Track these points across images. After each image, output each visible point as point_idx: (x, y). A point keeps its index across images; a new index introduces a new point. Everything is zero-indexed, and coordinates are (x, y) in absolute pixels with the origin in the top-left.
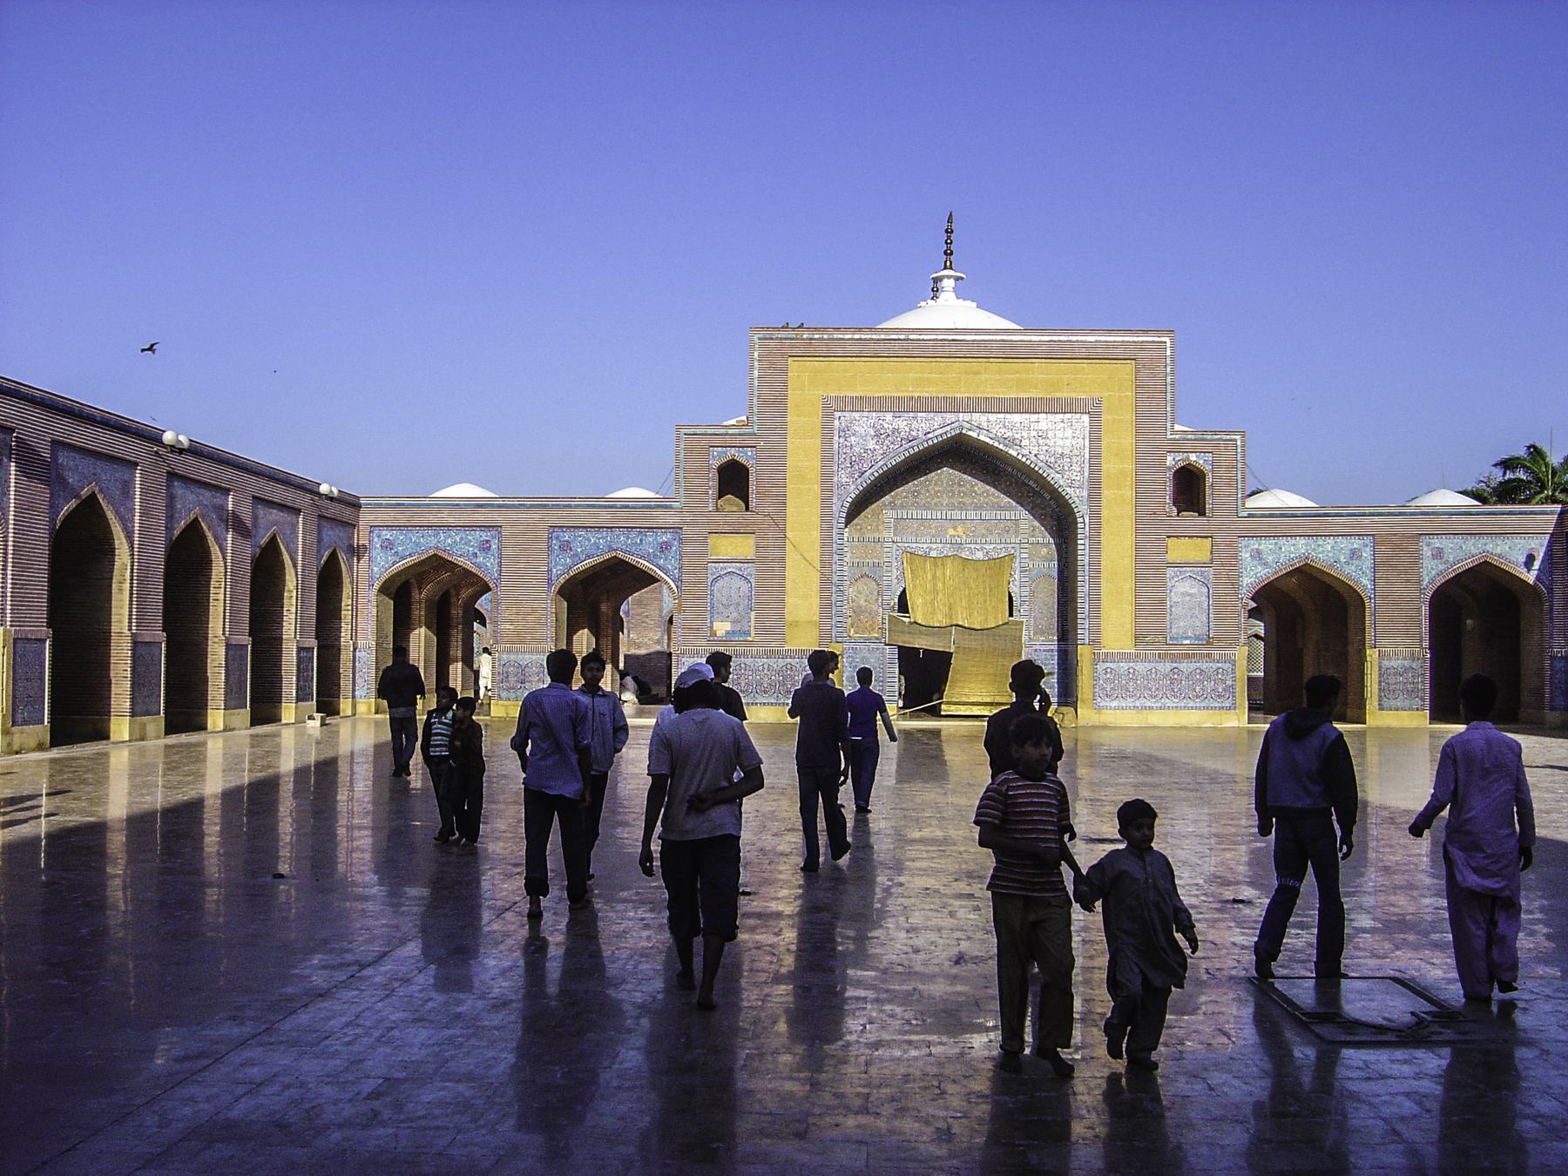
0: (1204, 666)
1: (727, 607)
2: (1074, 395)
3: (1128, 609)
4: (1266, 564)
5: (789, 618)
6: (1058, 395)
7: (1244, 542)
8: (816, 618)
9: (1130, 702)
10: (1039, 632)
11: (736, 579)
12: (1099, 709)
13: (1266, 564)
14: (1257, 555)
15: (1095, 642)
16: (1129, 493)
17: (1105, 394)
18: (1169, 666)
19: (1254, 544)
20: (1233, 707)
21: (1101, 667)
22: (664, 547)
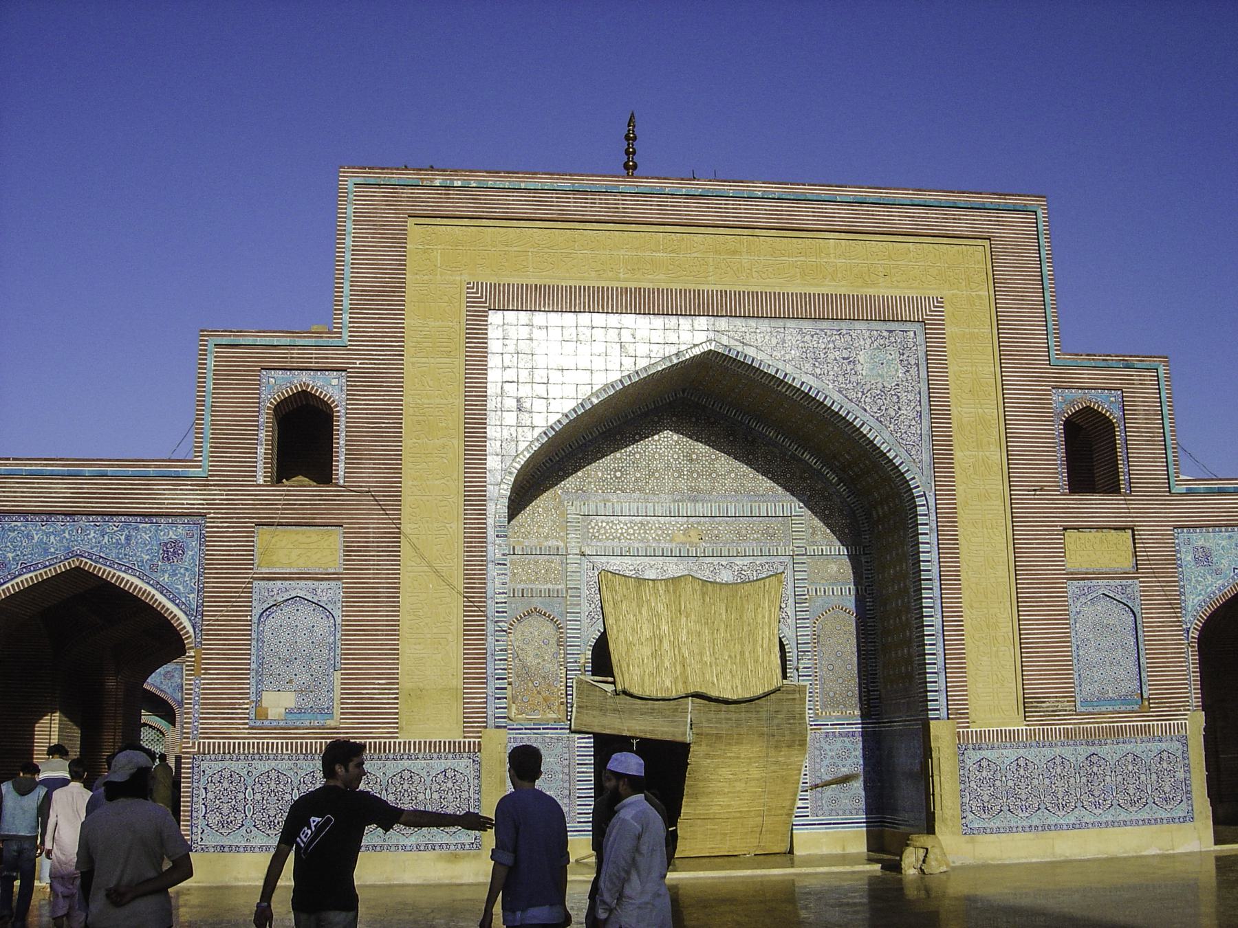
0: (1139, 748)
1: (287, 662)
2: (897, 293)
3: (1007, 656)
4: (1218, 572)
5: (405, 682)
6: (871, 291)
7: (1183, 536)
8: (457, 682)
9: (1021, 819)
10: (831, 702)
11: (308, 610)
12: (969, 831)
13: (1218, 572)
14: (1205, 558)
15: (958, 714)
16: (996, 456)
17: (946, 293)
18: (1084, 751)
19: (1200, 539)
20: (1190, 817)
21: (973, 756)
22: (172, 551)
